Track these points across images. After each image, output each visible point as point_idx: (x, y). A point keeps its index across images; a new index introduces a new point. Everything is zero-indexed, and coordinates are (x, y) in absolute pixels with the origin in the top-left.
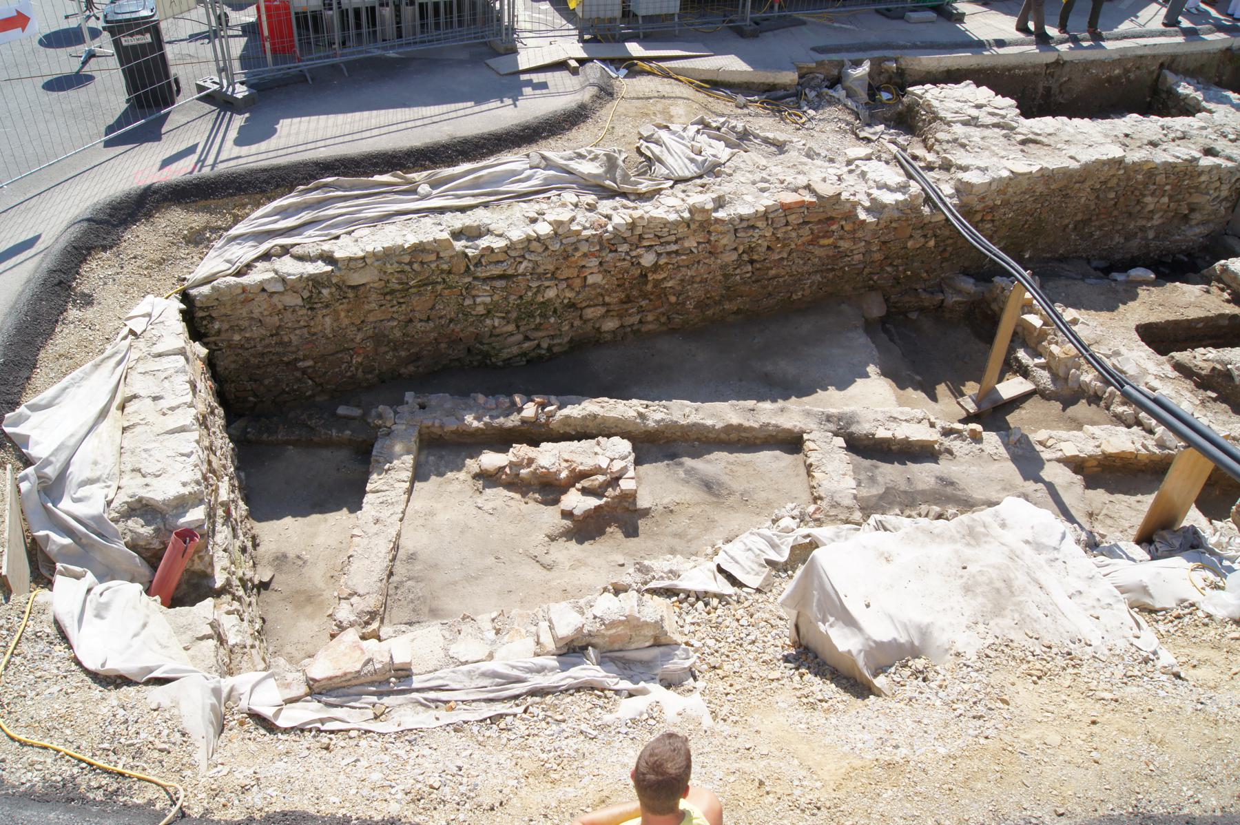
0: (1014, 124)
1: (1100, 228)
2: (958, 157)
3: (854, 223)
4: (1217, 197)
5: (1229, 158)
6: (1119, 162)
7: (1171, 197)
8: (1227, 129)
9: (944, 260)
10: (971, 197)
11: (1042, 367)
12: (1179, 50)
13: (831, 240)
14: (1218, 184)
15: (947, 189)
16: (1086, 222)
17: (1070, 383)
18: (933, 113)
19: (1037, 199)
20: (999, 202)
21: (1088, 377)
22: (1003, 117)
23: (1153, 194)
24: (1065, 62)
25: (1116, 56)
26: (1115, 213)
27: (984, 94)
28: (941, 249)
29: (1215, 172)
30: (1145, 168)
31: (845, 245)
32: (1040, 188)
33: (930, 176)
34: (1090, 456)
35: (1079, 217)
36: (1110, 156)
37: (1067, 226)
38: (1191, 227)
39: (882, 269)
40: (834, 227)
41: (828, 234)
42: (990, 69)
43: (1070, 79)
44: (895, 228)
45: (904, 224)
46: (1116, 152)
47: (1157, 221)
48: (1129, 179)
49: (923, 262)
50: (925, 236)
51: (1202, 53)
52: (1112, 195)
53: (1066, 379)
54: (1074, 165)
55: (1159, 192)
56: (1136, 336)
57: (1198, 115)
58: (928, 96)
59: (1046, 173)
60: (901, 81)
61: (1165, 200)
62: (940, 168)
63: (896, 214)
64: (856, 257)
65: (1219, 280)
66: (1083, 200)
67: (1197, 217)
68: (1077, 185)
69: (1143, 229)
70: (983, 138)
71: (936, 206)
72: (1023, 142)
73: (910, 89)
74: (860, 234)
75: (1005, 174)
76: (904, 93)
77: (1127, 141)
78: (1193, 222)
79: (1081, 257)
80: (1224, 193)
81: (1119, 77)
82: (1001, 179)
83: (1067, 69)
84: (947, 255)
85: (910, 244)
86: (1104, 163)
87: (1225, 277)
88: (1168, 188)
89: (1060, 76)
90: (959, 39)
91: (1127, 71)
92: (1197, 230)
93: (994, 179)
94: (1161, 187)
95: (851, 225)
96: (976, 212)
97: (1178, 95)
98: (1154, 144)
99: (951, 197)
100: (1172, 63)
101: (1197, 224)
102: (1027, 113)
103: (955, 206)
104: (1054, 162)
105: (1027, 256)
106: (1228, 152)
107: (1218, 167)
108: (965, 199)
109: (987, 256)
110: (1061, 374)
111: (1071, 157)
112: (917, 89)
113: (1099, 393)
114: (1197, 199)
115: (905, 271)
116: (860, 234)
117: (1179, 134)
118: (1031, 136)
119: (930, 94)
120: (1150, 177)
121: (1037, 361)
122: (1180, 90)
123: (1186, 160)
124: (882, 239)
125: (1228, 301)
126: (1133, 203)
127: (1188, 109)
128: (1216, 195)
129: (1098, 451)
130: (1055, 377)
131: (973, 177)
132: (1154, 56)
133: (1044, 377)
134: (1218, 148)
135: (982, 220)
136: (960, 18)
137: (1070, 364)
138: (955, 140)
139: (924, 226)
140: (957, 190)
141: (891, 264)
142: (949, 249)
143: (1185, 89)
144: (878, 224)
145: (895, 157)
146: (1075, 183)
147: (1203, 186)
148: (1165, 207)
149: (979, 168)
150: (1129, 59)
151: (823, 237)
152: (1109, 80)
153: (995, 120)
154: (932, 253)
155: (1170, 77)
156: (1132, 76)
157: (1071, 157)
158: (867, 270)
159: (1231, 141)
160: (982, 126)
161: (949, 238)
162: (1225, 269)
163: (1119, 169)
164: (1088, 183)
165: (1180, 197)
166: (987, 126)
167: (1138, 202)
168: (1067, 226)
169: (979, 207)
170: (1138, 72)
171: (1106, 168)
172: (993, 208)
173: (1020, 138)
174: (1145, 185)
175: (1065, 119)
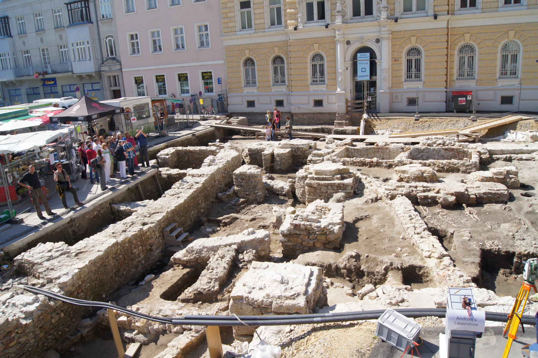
0: (69, 250)
1: (124, 270)
2: (53, 275)
3: (22, 327)
4: (156, 237)
5: (152, 223)
6: (117, 243)
7: (142, 246)
8: (145, 214)
9: (72, 318)
10: (68, 287)
11: (138, 334)
12: (113, 196)
13: (15, 342)
14: (154, 233)
15: (56, 290)
16: (118, 271)
17: (152, 333)
18: (31, 263)
19: (96, 272)
20: (80, 283)
21: (157, 326)
22: (62, 250)
23: (135, 248)
24: (74, 219)
25: (92, 208)
26: (126, 262)
27: (49, 245)
28: (68, 315)
29: (150, 230)
30: (127, 241)
31: (23, 340)
32: (93, 269)
33: (45, 289)
34: (177, 354)
35: (114, 271)
36: (112, 243)
37: (112, 276)
38: (154, 252)
39: (47, 339)
40: (13, 335)
41: (12, 340)
42: (45, 235)
43: (80, 224)
44: (43, 318)
45: (45, 314)
46: (113, 241)
47: (142, 256)
48: (124, 247)
49: (63, 325)
50: (58, 314)
51: (121, 194)
52: (121, 256)
53: (149, 332)
54: (101, 253)
55: (137, 246)
56: (163, 300)
57: (133, 214)
58: (25, 257)
59: (92, 262)
60: (9, 257)
61: (140, 247)
62: (48, 283)
63: (39, 313)
64: (32, 341)
65: (176, 264)
66: (112, 264)
67: (154, 247)
68: (107, 260)
69: (139, 262)
70: (59, 262)
71: (55, 299)
72: (76, 255)
73: (15, 258)
74: (27, 331)
75: (77, 271)
76: (14, 261)
77: (114, 235)
78: (154, 250)
79: (124, 285)
80: (158, 235)
81: (97, 215)
82: (76, 274)
83: (76, 220)
84: (72, 316)
85: (53, 321)
86: (111, 247)
87: (176, 262)
88: (139, 243)
89: (75, 224)
90: (26, 230)
91: (99, 211)
92: (157, 252)
93: (73, 276)
94: (136, 244)
95: (21, 329)
96: (74, 292)
97: (122, 211)
98: (124, 231)
99: (59, 292)
100: (113, 202)
101: (156, 250)
102: (71, 244)
103: (63, 294)
104: (93, 256)
105: (104, 296)
106: (150, 221)
107: (150, 227)
108: (66, 289)
109: (89, 306)
110: (146, 331)
111: (98, 251)
112: (19, 257)
113: (164, 329)
114: (150, 241)
115: (58, 333)
116: (27, 331)
117: (131, 224)
118: (78, 251)
119: (26, 256)
120: (130, 243)
121: (134, 333)
122: (122, 209)
123: (139, 231)
124: (39, 326)
125: (183, 269)
126: (130, 255)
127: (128, 214)
128: (155, 237)
129: (179, 350)
130: (145, 334)
131: (64, 279)
132: (105, 202)
133: (141, 337)
134: (146, 222)
135: (78, 293)
136: (22, 221)
137: (147, 326)
138: (48, 269)
139: (54, 310)
140: (60, 288)
141: (50, 334)
142: (71, 313)
143: (123, 208)
144: (33, 321)
145: (25, 289)
146: (106, 259)
147: (150, 236)
148: (142, 250)
149: (64, 274)
150: (97, 207)
151: (10, 342)
152: (94, 217)
153: (60, 253)
154: (65, 318)
155: (116, 206)
156: (102, 212)
157: (98, 251)
158: (40, 344)
159: (148, 217)
160: (56, 257)
161: (68, 308)
162: (175, 259)
163: (118, 246)
164: (110, 257)
165: (144, 244)
166: (58, 257)
167: (132, 253)
168: (112, 276)
169: (74, 289)
170: (103, 210)
171: (113, 248)
172: (80, 286)
173: (74, 254)
174: (131, 246)
175: (87, 239)
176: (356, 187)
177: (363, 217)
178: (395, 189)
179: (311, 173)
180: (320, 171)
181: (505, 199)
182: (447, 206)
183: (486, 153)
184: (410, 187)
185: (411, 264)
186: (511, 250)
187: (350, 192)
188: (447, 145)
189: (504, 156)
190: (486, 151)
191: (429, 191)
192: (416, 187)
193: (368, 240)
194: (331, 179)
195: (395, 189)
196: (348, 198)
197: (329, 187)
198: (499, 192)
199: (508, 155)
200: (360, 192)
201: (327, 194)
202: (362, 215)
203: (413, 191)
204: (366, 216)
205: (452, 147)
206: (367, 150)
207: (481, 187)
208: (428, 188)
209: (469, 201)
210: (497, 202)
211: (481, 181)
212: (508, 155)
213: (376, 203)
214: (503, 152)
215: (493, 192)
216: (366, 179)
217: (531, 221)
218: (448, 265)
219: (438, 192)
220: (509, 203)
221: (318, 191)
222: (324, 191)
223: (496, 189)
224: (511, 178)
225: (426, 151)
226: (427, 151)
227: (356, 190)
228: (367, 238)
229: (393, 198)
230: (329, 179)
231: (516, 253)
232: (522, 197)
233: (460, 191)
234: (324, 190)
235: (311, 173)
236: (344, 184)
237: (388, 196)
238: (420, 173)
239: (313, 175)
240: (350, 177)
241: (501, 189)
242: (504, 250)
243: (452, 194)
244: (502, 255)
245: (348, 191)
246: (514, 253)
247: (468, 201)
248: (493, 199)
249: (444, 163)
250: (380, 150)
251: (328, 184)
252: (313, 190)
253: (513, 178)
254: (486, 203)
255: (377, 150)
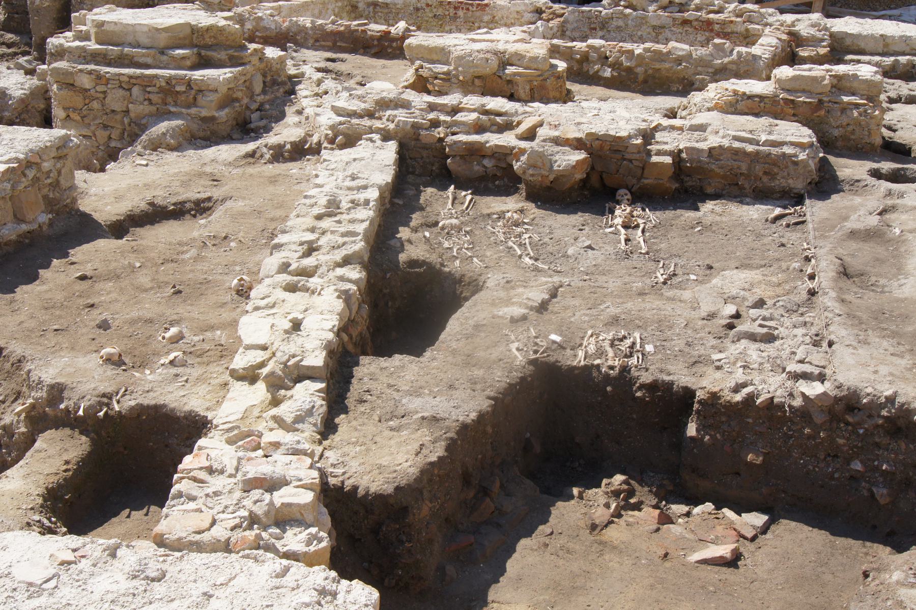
176: (254, 106)
177: (188, 205)
178: (370, 115)
179: (85, 37)
180: (116, 29)
181: (798, 185)
182: (549, 189)
183: (823, 40)
184: (432, 107)
185: (148, 400)
186: (681, 377)
187: (213, 119)
188: (698, 9)
189: (889, 60)
190: (819, 35)
191: (508, 127)
192: (455, 110)
193: (85, 285)
194: (149, 60)
195: (370, 115)
196: (205, 139)
197: (136, 90)
198: (775, 151)
199: (903, 59)
200: (262, 123)
201: (126, 121)
202: (180, 198)
203: (435, 124)
204: (198, 203)
205: (711, 16)
206: (417, 9)
207: (709, 129)
208: (499, 119)
209: (642, 177)
210: (762, 195)
211: (727, 113)
212: (903, 59)
213: (290, 165)
214: (886, 45)
215: (750, 148)
216: (319, 83)
217: (843, 266)
218: (289, 419)
219: (530, 135)
220: (807, 202)
221: (95, 105)
222: (118, 107)
223: (763, 138)
224: (846, 109)
225: (615, 23)
226: (621, 23)
227: (255, 116)
228: (83, 278)
229: (350, 141)
230: (142, 60)
231: (700, 395)
232: (873, 181)
233: (612, 133)
234: (115, 100)
235: (85, 37)
236: (189, 83)
237: (336, 137)
238: (494, 63)
239: (93, 45)
240: (234, 62)
241: (788, 139)
242: (646, 378)
243: (578, 144)
244: (635, 399)
245: (205, 113)
246: (689, 394)
247: (639, 179)
248: (747, 176)
249: (637, 52)
250: (461, 13)
251: (131, 77)
252: (78, 101)
253: (857, 106)
254: (715, 197)
255: (452, 11)
